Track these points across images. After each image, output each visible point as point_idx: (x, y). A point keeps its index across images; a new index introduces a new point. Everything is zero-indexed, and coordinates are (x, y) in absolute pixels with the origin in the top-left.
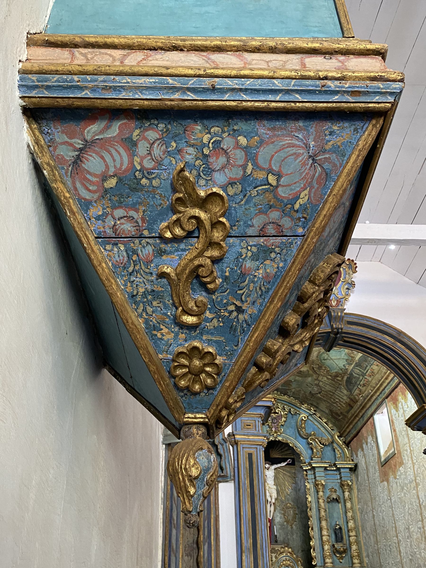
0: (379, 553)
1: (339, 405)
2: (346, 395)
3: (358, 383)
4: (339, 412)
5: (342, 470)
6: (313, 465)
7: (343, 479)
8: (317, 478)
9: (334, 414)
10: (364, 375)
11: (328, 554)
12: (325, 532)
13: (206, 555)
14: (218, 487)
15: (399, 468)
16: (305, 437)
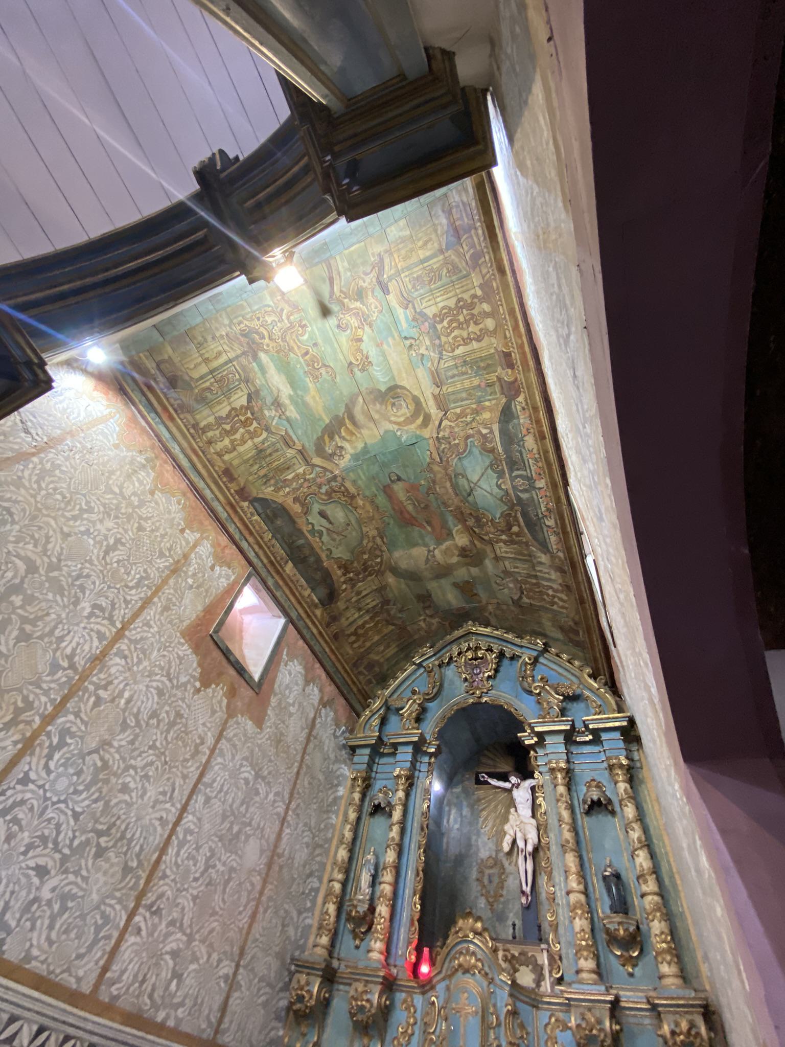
1: (561, 604)
3: (540, 516)
5: (604, 736)
6: (536, 729)
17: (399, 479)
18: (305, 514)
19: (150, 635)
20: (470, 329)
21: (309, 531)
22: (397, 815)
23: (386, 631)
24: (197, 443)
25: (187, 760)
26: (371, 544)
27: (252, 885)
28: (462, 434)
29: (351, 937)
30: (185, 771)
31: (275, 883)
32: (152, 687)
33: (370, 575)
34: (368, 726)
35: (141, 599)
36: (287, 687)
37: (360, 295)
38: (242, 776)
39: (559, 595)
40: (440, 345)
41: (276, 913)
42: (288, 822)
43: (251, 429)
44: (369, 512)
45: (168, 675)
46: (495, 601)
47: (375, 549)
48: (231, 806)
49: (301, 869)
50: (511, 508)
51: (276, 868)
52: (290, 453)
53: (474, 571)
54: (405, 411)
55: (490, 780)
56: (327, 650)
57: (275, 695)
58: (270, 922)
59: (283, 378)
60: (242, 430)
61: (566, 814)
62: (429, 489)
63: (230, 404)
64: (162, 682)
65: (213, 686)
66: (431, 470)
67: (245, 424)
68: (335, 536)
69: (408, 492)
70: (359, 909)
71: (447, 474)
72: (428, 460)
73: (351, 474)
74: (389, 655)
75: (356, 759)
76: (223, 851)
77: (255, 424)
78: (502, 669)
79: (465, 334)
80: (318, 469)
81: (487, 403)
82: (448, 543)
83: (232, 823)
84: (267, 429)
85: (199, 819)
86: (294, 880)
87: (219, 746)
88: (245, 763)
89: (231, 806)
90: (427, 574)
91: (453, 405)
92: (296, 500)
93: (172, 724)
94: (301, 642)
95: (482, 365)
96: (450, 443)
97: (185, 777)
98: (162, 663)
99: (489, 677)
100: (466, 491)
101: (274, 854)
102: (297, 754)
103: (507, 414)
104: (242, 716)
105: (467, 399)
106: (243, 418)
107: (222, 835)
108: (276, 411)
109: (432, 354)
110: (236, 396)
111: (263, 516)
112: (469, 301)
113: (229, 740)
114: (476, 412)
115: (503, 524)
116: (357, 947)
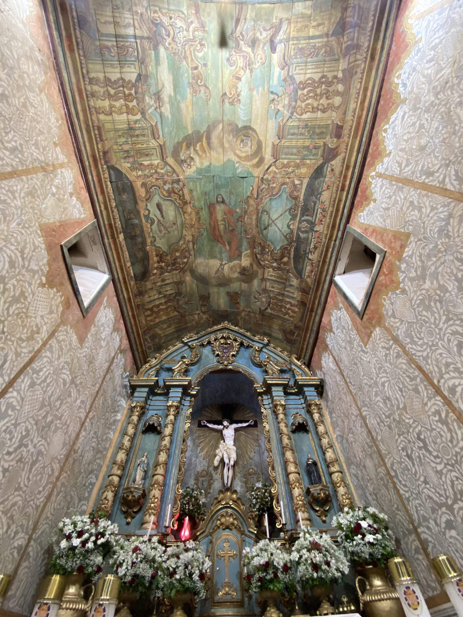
0: (391, 477)
1: (291, 314)
2: (297, 288)
3: (308, 251)
7: (308, 398)
8: (275, 398)
9: (288, 336)
10: (312, 224)
11: (300, 502)
12: (292, 468)
15: (400, 259)
17: (223, 202)
18: (147, 200)
19: (13, 204)
20: (321, 102)
21: (145, 216)
22: (168, 431)
23: (172, 315)
24: (85, 84)
25: (23, 341)
26: (184, 246)
27: (53, 470)
28: (280, 180)
29: (123, 516)
30: (19, 350)
31: (69, 473)
32: (6, 252)
34: (146, 375)
35: (12, 166)
36: (103, 325)
37: (254, 43)
38: (63, 376)
39: (293, 308)
40: (294, 107)
41: (65, 497)
42: (85, 427)
43: (131, 105)
44: (192, 220)
45: (22, 252)
46: (249, 309)
47: (186, 251)
48: (50, 398)
49: (86, 466)
50: (290, 244)
51: (71, 460)
52: (153, 143)
53: (244, 286)
54: (248, 149)
55: (208, 425)
56: (130, 314)
57: (95, 326)
58: (60, 504)
59: (171, 78)
60: (122, 101)
62: (241, 217)
63: (121, 73)
64: (15, 254)
65: (55, 290)
66: (247, 202)
67: (127, 98)
68: (162, 228)
69: (225, 214)
70: (134, 494)
71: (257, 209)
72: (249, 194)
73: (191, 184)
74: (168, 333)
75: (136, 394)
76: (36, 435)
77: (135, 103)
78: (240, 352)
79: (315, 105)
80: (169, 168)
81: (308, 162)
82: (235, 262)
83: (48, 413)
84: (143, 113)
85: (22, 399)
86: (80, 473)
87: (50, 342)
88: (66, 367)
89: (50, 398)
90: (214, 281)
91: (283, 156)
92: (144, 185)
93: (16, 300)
94: (115, 299)
95: (317, 131)
96: (269, 185)
97: (18, 354)
98: (19, 238)
99: (233, 355)
100: (264, 225)
101: (72, 450)
102: (99, 378)
103: (318, 172)
104: (71, 328)
105: (295, 155)
106: (127, 92)
107: (38, 420)
108: (155, 102)
109: (285, 112)
110: (129, 70)
111: (114, 184)
112: (330, 80)
113: (59, 342)
114: (298, 166)
115: (279, 255)
116: (128, 524)
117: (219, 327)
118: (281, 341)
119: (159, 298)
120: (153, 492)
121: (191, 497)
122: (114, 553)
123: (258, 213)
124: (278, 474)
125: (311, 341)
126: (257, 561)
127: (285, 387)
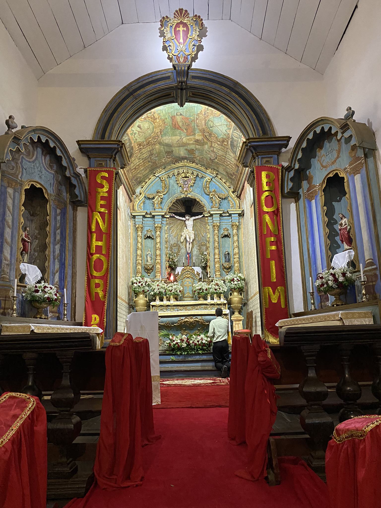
4: (232, 173)
5: (233, 215)
6: (211, 213)
12: (217, 256)
13: (57, 252)
14: (77, 210)
16: (208, 194)
17: (181, 115)
22: (158, 240)
33: (149, 146)
61: (217, 239)
68: (141, 133)
75: (136, 220)
82: (191, 137)
117: (181, 164)
118: (225, 176)
119: (139, 162)
120: (157, 266)
121: (170, 258)
122: (151, 286)
123: (206, 120)
124: (211, 258)
125: (241, 187)
126: (197, 288)
127: (221, 215)
